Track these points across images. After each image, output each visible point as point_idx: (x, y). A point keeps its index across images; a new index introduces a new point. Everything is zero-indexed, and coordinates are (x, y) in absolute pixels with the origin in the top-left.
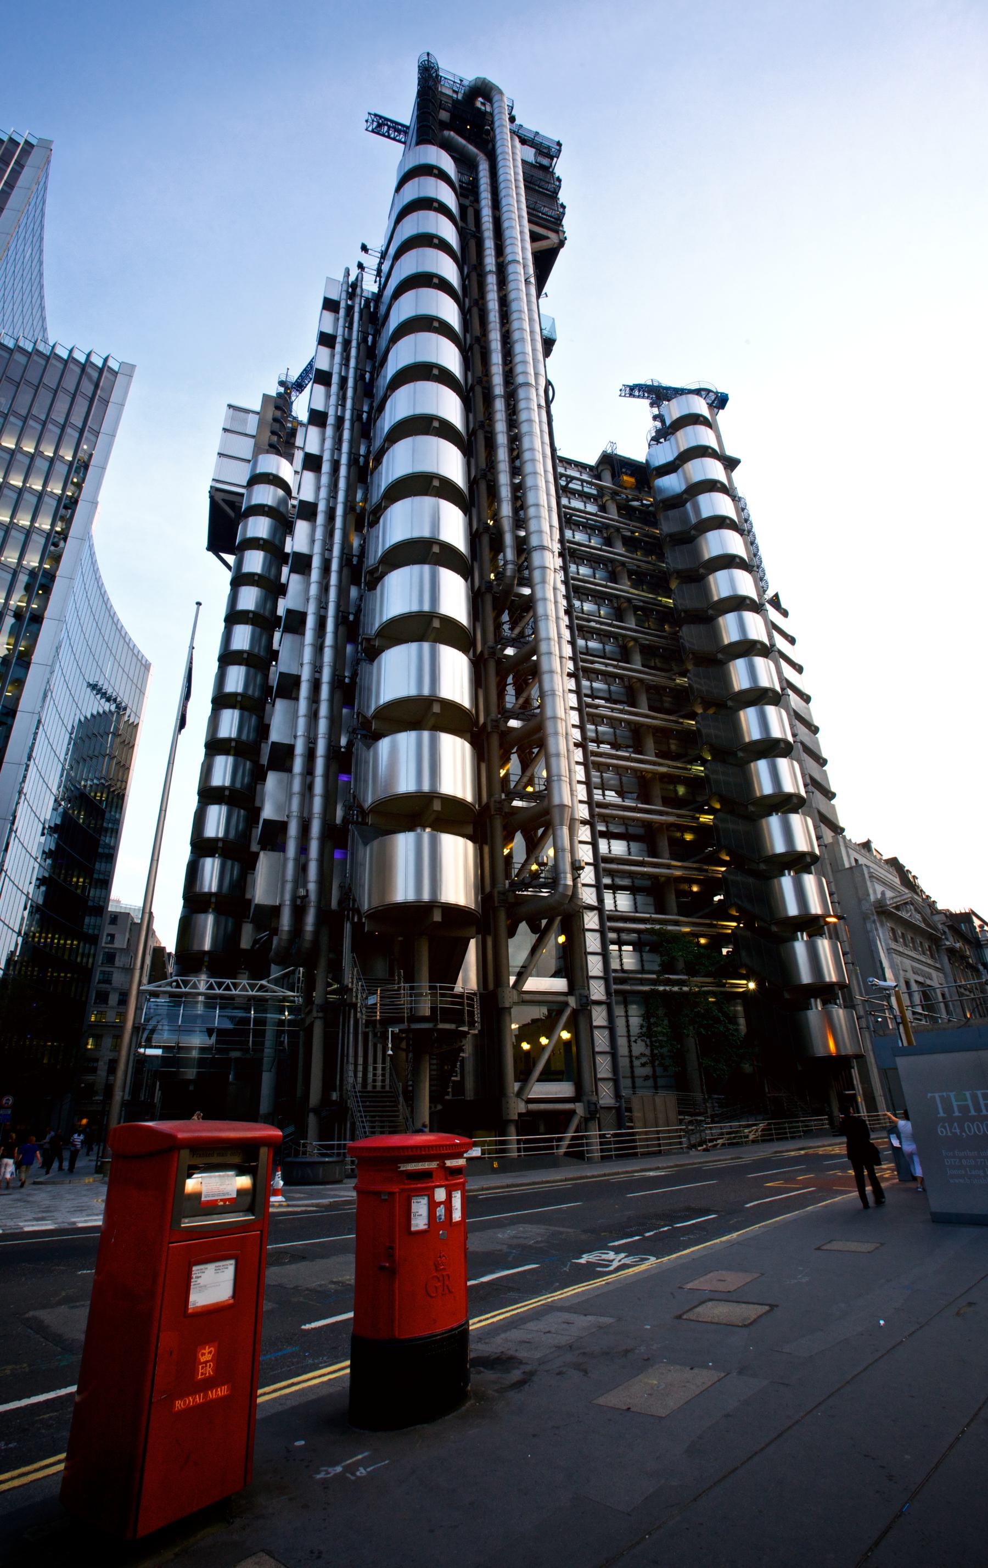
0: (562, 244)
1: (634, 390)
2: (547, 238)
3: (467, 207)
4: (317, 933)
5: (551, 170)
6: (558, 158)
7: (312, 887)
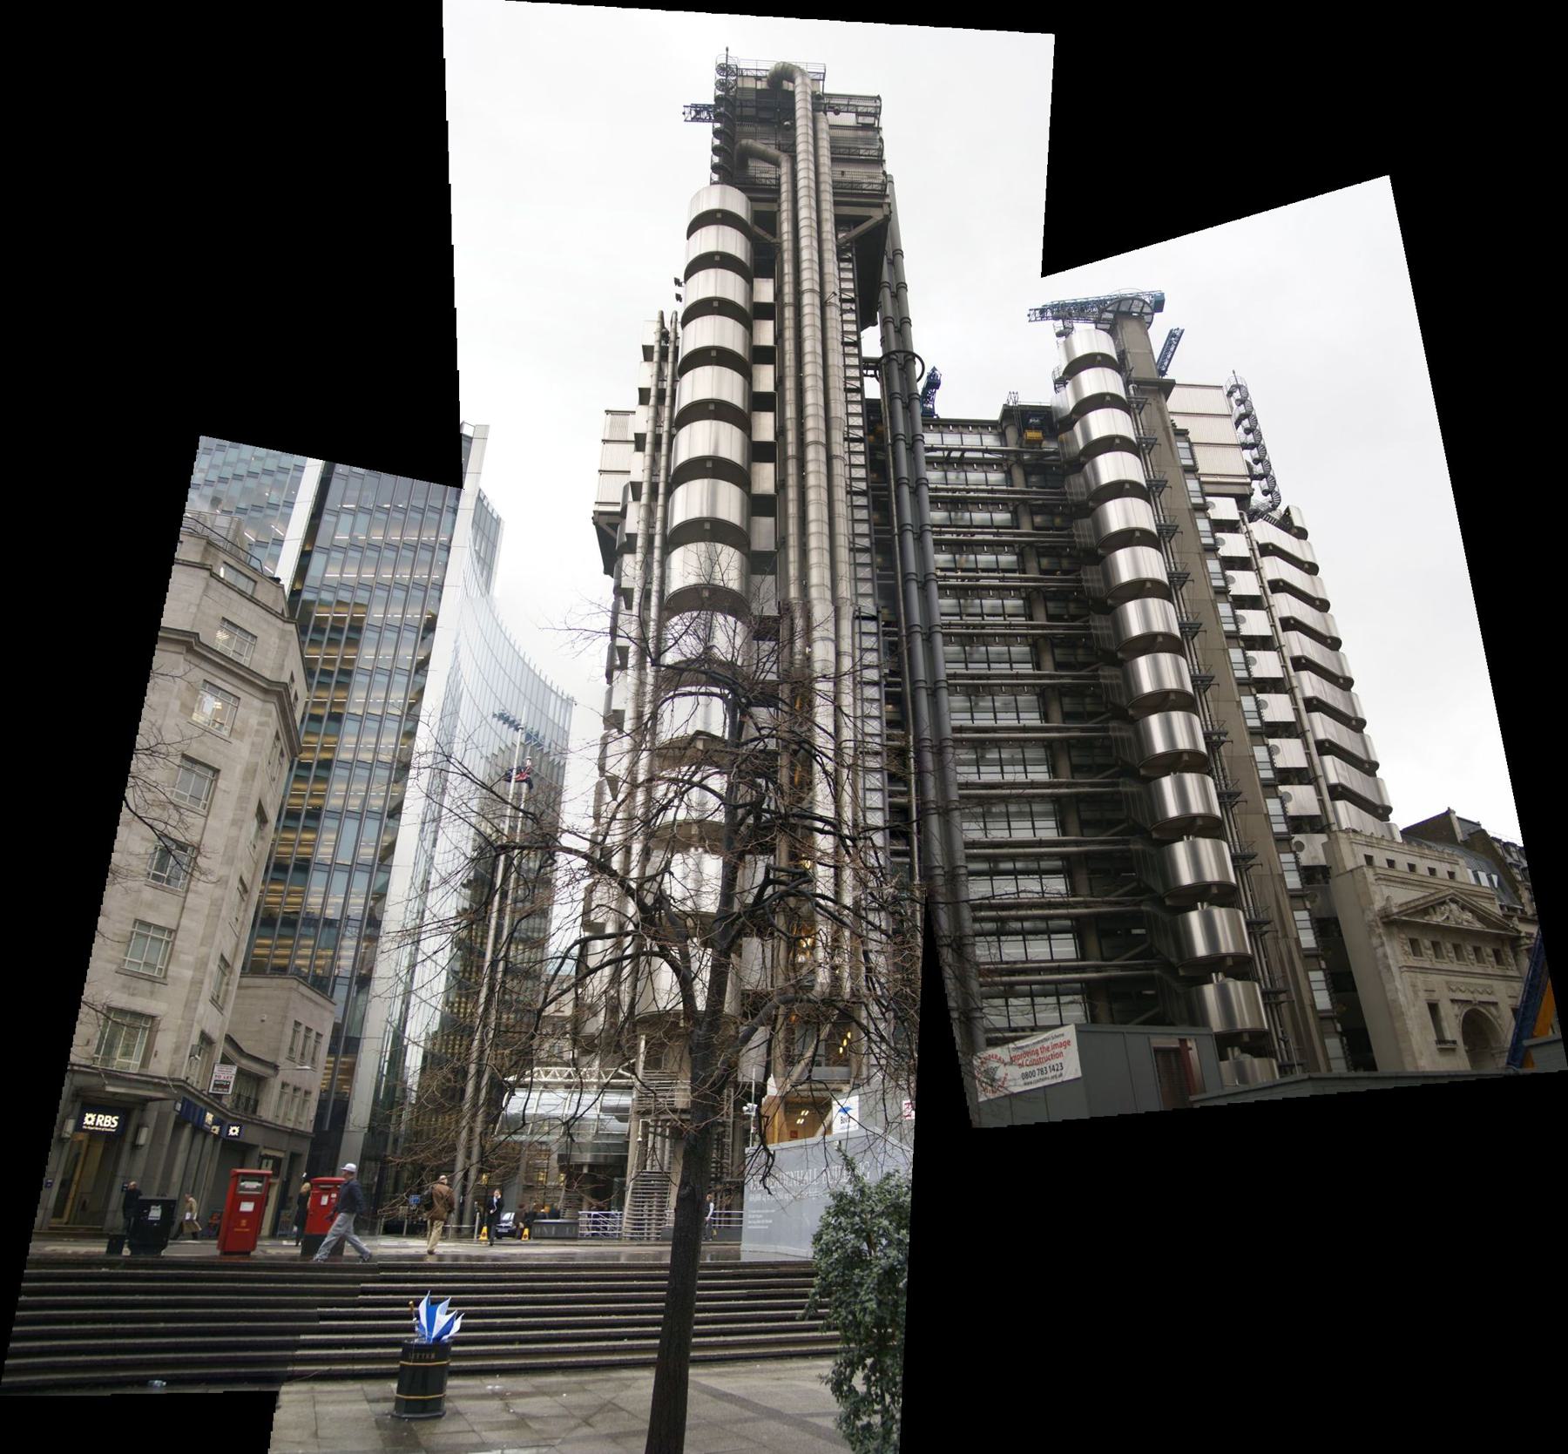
2: (870, 217)
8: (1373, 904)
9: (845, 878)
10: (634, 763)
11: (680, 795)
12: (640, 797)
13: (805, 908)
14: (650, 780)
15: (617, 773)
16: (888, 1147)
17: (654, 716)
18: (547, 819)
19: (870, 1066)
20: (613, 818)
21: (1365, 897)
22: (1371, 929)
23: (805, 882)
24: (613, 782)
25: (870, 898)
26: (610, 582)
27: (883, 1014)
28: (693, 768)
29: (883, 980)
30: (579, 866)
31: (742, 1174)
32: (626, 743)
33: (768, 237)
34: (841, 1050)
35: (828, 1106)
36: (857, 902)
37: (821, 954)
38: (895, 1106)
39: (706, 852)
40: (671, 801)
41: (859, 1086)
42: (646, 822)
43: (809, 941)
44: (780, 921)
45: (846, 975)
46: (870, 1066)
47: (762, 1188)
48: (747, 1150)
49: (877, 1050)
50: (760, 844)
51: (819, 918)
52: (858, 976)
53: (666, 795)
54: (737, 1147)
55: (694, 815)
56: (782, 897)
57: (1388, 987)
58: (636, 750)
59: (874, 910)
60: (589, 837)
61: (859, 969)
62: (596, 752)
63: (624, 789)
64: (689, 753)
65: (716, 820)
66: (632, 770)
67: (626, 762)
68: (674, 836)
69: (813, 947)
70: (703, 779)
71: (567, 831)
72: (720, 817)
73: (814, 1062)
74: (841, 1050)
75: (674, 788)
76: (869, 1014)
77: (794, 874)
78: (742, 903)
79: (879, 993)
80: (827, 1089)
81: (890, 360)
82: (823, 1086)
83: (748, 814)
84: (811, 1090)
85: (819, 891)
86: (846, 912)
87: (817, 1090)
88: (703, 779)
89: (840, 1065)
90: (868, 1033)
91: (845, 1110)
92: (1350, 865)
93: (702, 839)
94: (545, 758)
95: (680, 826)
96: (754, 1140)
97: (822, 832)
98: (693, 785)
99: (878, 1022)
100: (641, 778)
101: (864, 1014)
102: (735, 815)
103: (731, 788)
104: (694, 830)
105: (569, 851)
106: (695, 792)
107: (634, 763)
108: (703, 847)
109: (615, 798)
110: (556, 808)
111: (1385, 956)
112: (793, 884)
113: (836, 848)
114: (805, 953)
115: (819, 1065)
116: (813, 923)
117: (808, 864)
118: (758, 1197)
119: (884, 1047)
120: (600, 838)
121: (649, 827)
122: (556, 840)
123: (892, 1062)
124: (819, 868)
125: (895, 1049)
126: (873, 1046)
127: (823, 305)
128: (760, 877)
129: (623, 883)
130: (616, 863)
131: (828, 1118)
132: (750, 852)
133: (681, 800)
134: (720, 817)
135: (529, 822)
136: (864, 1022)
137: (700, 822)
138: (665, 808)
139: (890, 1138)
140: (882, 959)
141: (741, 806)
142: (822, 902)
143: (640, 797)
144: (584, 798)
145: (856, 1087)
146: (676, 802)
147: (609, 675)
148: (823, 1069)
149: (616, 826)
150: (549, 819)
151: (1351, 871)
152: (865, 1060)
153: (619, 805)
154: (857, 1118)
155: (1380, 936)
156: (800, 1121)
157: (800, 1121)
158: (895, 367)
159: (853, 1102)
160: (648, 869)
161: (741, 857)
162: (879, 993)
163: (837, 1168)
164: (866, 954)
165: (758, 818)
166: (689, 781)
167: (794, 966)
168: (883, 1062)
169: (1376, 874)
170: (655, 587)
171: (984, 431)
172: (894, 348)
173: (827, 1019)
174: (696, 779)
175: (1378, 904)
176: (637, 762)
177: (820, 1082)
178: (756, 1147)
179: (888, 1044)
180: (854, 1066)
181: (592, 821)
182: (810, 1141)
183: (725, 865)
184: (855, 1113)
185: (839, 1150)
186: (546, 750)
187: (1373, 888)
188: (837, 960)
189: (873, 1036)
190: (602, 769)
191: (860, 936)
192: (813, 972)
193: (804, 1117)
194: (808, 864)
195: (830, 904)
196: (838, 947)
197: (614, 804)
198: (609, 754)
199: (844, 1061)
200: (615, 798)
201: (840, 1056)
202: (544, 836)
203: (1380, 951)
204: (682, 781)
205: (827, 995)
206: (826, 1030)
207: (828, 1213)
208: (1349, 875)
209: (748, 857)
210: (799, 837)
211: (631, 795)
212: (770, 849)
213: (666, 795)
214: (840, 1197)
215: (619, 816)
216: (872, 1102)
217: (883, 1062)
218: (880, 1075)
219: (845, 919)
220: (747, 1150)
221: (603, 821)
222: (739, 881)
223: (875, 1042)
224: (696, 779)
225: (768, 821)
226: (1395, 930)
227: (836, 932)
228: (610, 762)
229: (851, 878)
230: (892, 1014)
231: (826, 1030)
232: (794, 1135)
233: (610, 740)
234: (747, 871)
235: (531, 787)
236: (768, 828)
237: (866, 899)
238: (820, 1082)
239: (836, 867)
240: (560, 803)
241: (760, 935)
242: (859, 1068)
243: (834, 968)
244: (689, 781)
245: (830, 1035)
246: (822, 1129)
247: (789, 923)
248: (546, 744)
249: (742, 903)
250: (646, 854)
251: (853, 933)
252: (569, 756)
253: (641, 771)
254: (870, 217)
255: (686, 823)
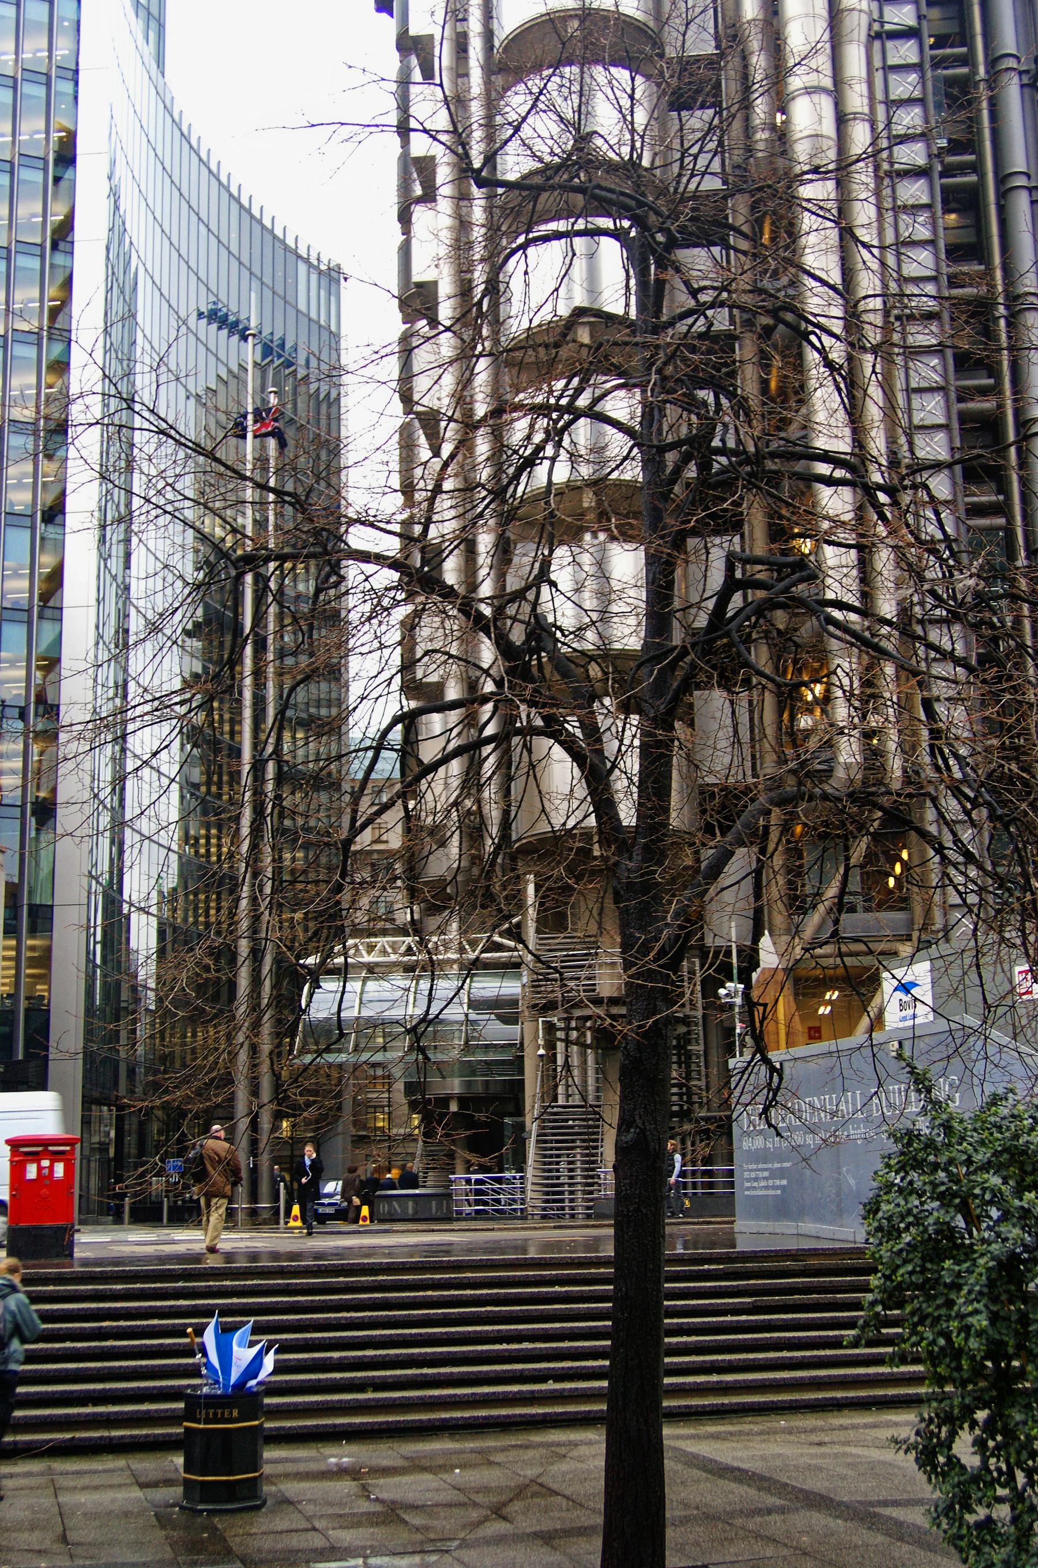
9: (879, 566)
10: (465, 382)
11: (554, 435)
12: (483, 447)
13: (808, 628)
14: (497, 413)
15: (435, 404)
16: (991, 1050)
17: (494, 288)
18: (318, 503)
19: (947, 908)
20: (437, 490)
23: (802, 580)
24: (430, 421)
25: (929, 600)
26: (388, 26)
27: (967, 813)
28: (576, 381)
29: (963, 751)
30: (386, 583)
31: (726, 1104)
32: (447, 345)
34: (891, 882)
35: (875, 982)
36: (904, 610)
37: (841, 712)
38: (1000, 977)
39: (613, 538)
40: (540, 448)
41: (929, 944)
42: (498, 493)
43: (818, 689)
44: (761, 656)
45: (892, 746)
46: (947, 908)
47: (763, 1126)
48: (732, 1063)
49: (961, 879)
50: (713, 516)
51: (834, 645)
52: (914, 747)
53: (529, 437)
54: (714, 1058)
55: (585, 471)
56: (761, 610)
58: (465, 356)
59: (940, 621)
60: (397, 528)
61: (915, 733)
62: (392, 368)
63: (451, 432)
64: (564, 352)
65: (627, 476)
66: (462, 397)
67: (449, 381)
68: (552, 515)
69: (827, 699)
70: (596, 401)
71: (358, 521)
72: (633, 472)
73: (841, 906)
74: (891, 882)
75: (542, 423)
76: (941, 815)
77: (780, 567)
78: (687, 627)
79: (958, 775)
80: (871, 952)
82: (861, 947)
83: (686, 459)
84: (841, 955)
85: (830, 595)
86: (885, 630)
87: (851, 954)
88: (596, 401)
89: (891, 908)
90: (940, 850)
91: (905, 988)
93: (603, 516)
94: (302, 389)
95: (560, 494)
96: (743, 1045)
97: (830, 481)
98: (578, 414)
99: (958, 828)
100: (481, 410)
101: (930, 814)
102: (661, 465)
103: (651, 413)
104: (588, 500)
105: (365, 557)
106: (583, 431)
107: (465, 382)
108: (608, 530)
109: (436, 453)
110: (334, 480)
112: (781, 585)
113: (859, 509)
114: (811, 712)
115: (852, 909)
116: (823, 656)
117: (807, 546)
118: (759, 1142)
119: (973, 873)
120: (418, 529)
121: (504, 501)
122: (340, 539)
123: (990, 899)
124: (829, 551)
125: (995, 876)
126: (952, 871)
128: (717, 579)
129: (467, 607)
130: (451, 572)
131: (876, 1002)
132: (694, 532)
133: (559, 445)
134: (633, 472)
135: (289, 510)
136: (933, 829)
137: (597, 484)
138: (530, 463)
139: (995, 1033)
140: (959, 713)
141: (672, 446)
142: (837, 614)
143: (483, 447)
144: (380, 456)
145: (923, 945)
146: (549, 451)
147: (405, 218)
148: (860, 916)
149: (444, 503)
150: (323, 502)
152: (937, 898)
153: (446, 465)
154: (929, 1000)
156: (824, 1010)
157: (824, 1010)
159: (921, 971)
160: (509, 579)
161: (679, 542)
162: (958, 775)
163: (896, 1090)
164: (928, 705)
165: (704, 467)
166: (570, 408)
167: (795, 738)
168: (972, 899)
170: (475, 25)
173: (861, 827)
174: (583, 402)
176: (469, 381)
177: (856, 940)
178: (747, 1057)
179: (980, 867)
180: (918, 910)
181: (399, 499)
182: (845, 1043)
183: (651, 560)
184: (924, 992)
185: (900, 1057)
186: (301, 373)
188: (874, 721)
189: (951, 854)
190: (407, 398)
191: (915, 673)
192: (829, 744)
193: (830, 1002)
194: (807, 546)
195: (853, 617)
196: (874, 696)
197: (436, 464)
198: (416, 369)
199: (899, 901)
200: (436, 453)
201: (891, 892)
202: (317, 533)
204: (557, 408)
205: (858, 784)
206: (860, 848)
207: (888, 1166)
209: (692, 542)
210: (785, 496)
211: (465, 444)
212: (733, 524)
213: (529, 437)
214: (911, 1136)
215: (447, 485)
216: (956, 971)
217: (972, 899)
218: (968, 923)
219: (884, 644)
220: (732, 1063)
221: (419, 496)
222: (679, 588)
223: (955, 865)
224: (583, 402)
225: (724, 470)
227: (869, 668)
228: (421, 384)
229: (890, 566)
230: (985, 812)
231: (860, 848)
232: (815, 1034)
233: (415, 342)
234: (692, 567)
235: (282, 444)
236: (726, 483)
237: (922, 603)
238: (856, 940)
239: (860, 548)
240: (339, 470)
241: (726, 684)
242: (928, 913)
243: (868, 735)
244: (570, 408)
245: (870, 857)
246: (865, 1022)
247: (777, 658)
248: (301, 361)
249: (687, 627)
250: (504, 551)
251: (900, 667)
252: (346, 379)
253: (480, 397)
255: (572, 488)
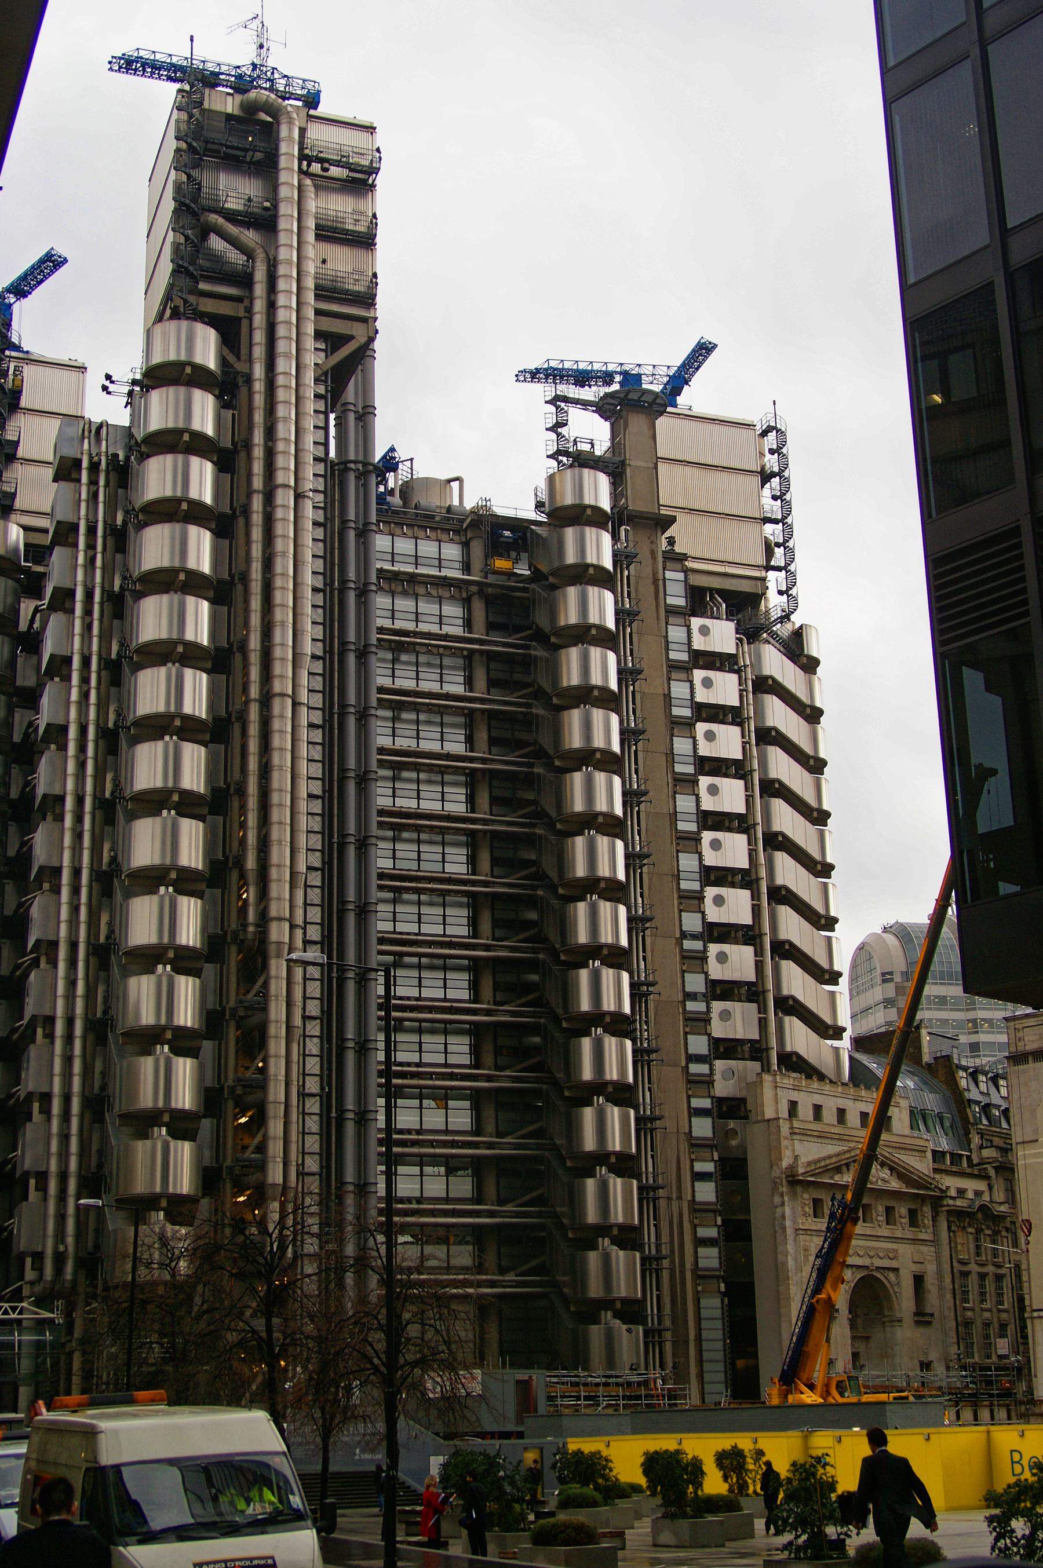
0: (372, 340)
1: (534, 375)
2: (351, 338)
3: (241, 318)
4: (74, 1281)
5: (370, 181)
6: (377, 174)
7: (70, 1240)
8: (781, 1160)
21: (774, 1151)
22: (775, 1184)
33: (231, 359)
57: (780, 1248)
81: (347, 470)
92: (769, 1113)
111: (783, 1217)
127: (299, 497)
151: (768, 1120)
155: (782, 1195)
158: (352, 477)
169: (792, 1128)
171: (444, 537)
172: (352, 457)
175: (785, 1163)
187: (784, 1143)
203: (779, 1210)
208: (766, 1124)
226: (799, 1189)
254: (351, 338)
